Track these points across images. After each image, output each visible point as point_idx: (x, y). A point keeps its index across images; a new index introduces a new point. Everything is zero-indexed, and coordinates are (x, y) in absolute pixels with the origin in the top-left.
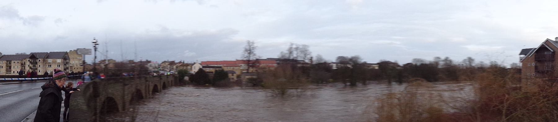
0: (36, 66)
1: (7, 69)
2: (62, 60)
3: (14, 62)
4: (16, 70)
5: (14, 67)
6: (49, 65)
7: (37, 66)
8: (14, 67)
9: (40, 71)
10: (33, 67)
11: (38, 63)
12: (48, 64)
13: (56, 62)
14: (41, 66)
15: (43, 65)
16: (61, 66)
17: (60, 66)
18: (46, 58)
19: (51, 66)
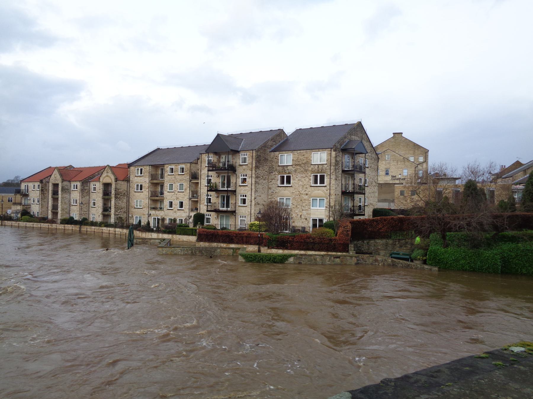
0: (233, 180)
2: (333, 153)
3: (172, 170)
4: (177, 198)
5: (171, 185)
6: (283, 178)
7: (236, 180)
8: (171, 185)
9: (244, 201)
10: (223, 184)
11: (239, 170)
12: (279, 173)
13: (308, 163)
14: (248, 180)
15: (257, 177)
16: (326, 180)
17: (322, 181)
18: (274, 151)
19: (289, 181)
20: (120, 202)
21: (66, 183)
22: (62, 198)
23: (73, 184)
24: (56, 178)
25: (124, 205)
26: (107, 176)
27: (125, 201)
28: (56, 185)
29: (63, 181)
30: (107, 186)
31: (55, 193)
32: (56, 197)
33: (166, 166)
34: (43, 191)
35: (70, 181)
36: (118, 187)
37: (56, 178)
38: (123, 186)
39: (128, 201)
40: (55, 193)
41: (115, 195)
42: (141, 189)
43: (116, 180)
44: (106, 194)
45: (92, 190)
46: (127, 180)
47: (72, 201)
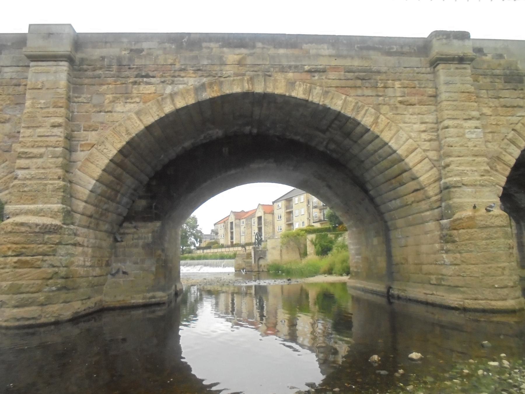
1: (287, 221)
20: (268, 229)
21: (237, 221)
22: (235, 230)
23: (241, 221)
24: (232, 219)
25: (271, 231)
26: (259, 211)
27: (271, 228)
28: (232, 223)
29: (236, 219)
30: (260, 218)
31: (232, 228)
32: (232, 231)
33: (293, 198)
34: (226, 229)
35: (240, 219)
36: (266, 218)
37: (232, 219)
38: (269, 217)
39: (274, 228)
40: (232, 228)
41: (264, 223)
42: (281, 218)
43: (265, 213)
44: (260, 223)
45: (253, 224)
46: (272, 213)
47: (241, 233)
